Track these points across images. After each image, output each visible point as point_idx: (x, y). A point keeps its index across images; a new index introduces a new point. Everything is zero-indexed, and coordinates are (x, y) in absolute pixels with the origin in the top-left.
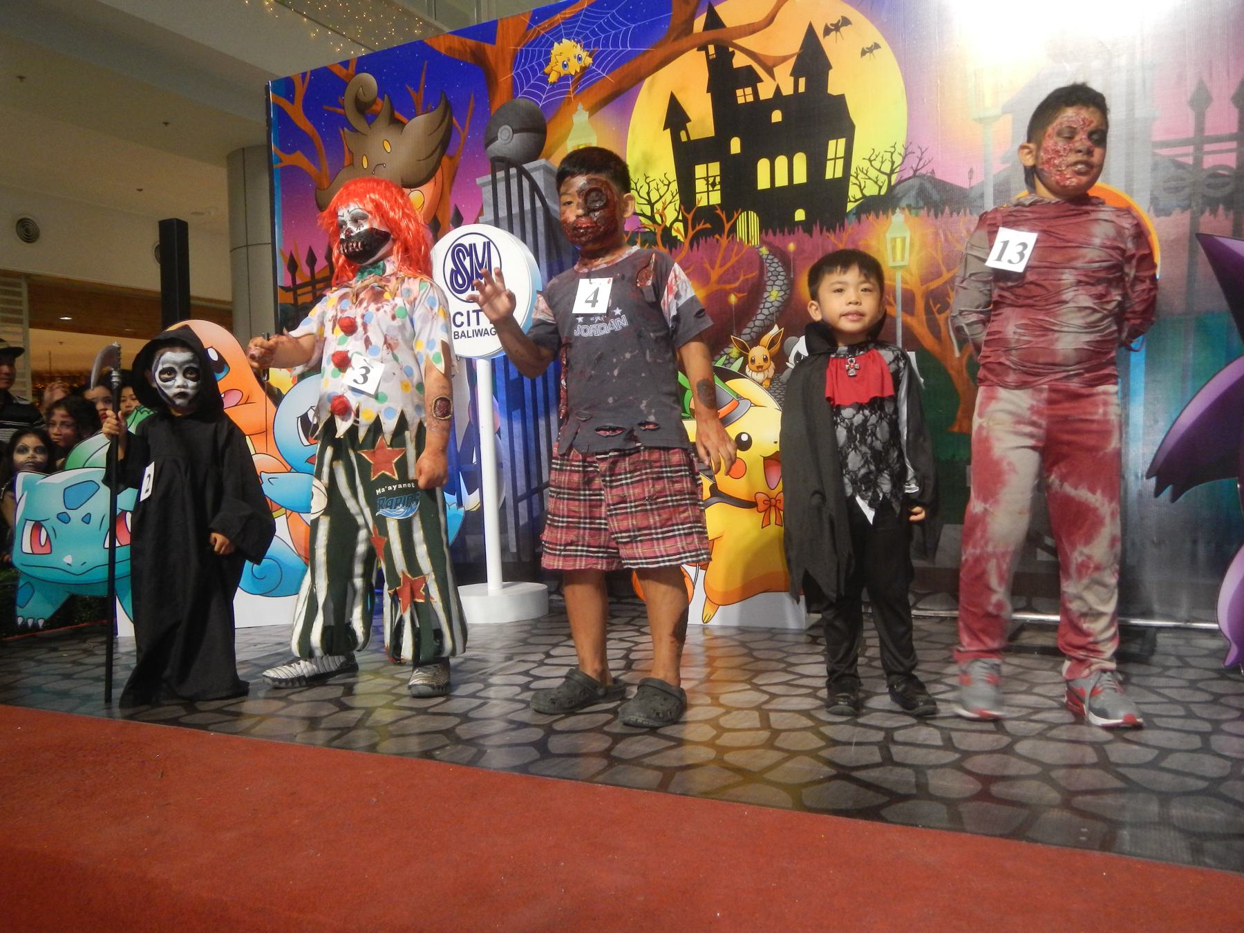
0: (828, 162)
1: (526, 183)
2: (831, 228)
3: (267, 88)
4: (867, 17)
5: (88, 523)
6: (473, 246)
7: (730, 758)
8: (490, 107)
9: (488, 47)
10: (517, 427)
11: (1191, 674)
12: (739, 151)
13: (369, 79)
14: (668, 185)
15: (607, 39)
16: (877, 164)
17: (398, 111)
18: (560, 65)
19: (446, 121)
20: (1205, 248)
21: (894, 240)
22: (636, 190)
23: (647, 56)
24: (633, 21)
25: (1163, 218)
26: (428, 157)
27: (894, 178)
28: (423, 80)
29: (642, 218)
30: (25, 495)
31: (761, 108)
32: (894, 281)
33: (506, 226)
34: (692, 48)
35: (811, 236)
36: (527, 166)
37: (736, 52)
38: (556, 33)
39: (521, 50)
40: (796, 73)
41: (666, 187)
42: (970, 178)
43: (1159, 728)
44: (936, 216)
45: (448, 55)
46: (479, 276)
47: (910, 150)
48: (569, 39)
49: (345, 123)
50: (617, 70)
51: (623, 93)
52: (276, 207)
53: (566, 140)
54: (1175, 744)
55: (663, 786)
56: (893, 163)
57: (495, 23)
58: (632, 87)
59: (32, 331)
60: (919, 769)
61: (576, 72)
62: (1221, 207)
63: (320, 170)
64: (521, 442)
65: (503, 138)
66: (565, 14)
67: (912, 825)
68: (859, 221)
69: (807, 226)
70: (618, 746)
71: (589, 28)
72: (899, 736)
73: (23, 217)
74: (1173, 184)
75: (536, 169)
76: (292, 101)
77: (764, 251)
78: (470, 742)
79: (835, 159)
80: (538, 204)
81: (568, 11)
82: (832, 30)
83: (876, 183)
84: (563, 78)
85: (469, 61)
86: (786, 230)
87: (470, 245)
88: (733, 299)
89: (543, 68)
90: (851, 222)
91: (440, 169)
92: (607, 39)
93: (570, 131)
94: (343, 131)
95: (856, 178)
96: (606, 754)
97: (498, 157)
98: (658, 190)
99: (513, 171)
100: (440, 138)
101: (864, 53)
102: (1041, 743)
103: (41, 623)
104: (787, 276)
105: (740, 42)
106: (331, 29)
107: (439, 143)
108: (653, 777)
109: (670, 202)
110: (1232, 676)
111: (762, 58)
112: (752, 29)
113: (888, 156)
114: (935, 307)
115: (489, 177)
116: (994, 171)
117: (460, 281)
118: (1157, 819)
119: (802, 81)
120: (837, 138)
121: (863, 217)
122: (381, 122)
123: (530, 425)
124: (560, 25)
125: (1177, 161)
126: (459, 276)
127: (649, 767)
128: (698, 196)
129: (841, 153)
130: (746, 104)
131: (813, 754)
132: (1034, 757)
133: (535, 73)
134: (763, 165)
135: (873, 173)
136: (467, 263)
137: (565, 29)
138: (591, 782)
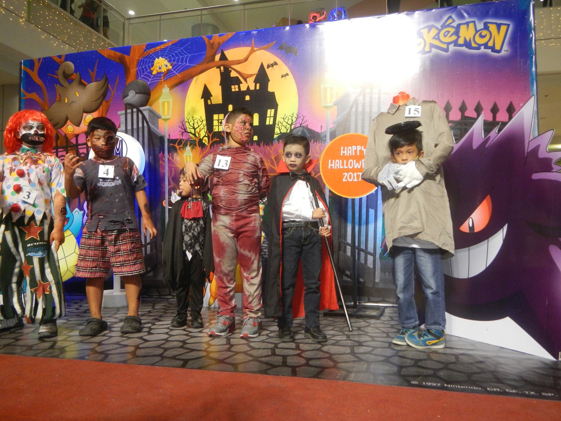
1: (140, 116)
2: (268, 144)
3: (21, 63)
4: (284, 63)
8: (126, 81)
9: (126, 56)
13: (71, 65)
14: (202, 122)
15: (179, 59)
16: (286, 120)
17: (83, 79)
18: (158, 68)
22: (188, 122)
23: (195, 68)
28: (96, 67)
29: (190, 135)
31: (241, 94)
33: (131, 133)
35: (260, 146)
36: (141, 108)
37: (232, 70)
38: (156, 55)
39: (141, 60)
40: (256, 82)
42: (321, 129)
43: (375, 341)
45: (108, 58)
47: (299, 116)
48: (162, 57)
49: (58, 82)
50: (182, 72)
51: (185, 81)
53: (158, 98)
56: (292, 120)
57: (130, 47)
58: (188, 79)
60: (285, 357)
61: (165, 71)
65: (131, 95)
66: (161, 47)
67: (278, 375)
68: (279, 143)
69: (258, 143)
70: (166, 352)
71: (171, 54)
72: (279, 346)
75: (145, 110)
76: (33, 70)
78: (102, 353)
79: (270, 117)
80: (145, 125)
82: (271, 66)
83: (286, 128)
85: (118, 62)
89: (150, 68)
90: (275, 142)
92: (179, 59)
93: (160, 96)
94: (57, 85)
96: (161, 355)
100: (102, 93)
101: (282, 77)
105: (234, 67)
106: (52, 35)
108: (181, 363)
111: (243, 74)
112: (239, 62)
115: (124, 112)
116: (330, 127)
119: (258, 85)
120: (271, 109)
122: (75, 84)
124: (158, 51)
128: (214, 127)
129: (272, 115)
130: (235, 92)
131: (245, 353)
132: (329, 352)
133: (147, 70)
135: (285, 124)
137: (161, 53)
138: (153, 365)
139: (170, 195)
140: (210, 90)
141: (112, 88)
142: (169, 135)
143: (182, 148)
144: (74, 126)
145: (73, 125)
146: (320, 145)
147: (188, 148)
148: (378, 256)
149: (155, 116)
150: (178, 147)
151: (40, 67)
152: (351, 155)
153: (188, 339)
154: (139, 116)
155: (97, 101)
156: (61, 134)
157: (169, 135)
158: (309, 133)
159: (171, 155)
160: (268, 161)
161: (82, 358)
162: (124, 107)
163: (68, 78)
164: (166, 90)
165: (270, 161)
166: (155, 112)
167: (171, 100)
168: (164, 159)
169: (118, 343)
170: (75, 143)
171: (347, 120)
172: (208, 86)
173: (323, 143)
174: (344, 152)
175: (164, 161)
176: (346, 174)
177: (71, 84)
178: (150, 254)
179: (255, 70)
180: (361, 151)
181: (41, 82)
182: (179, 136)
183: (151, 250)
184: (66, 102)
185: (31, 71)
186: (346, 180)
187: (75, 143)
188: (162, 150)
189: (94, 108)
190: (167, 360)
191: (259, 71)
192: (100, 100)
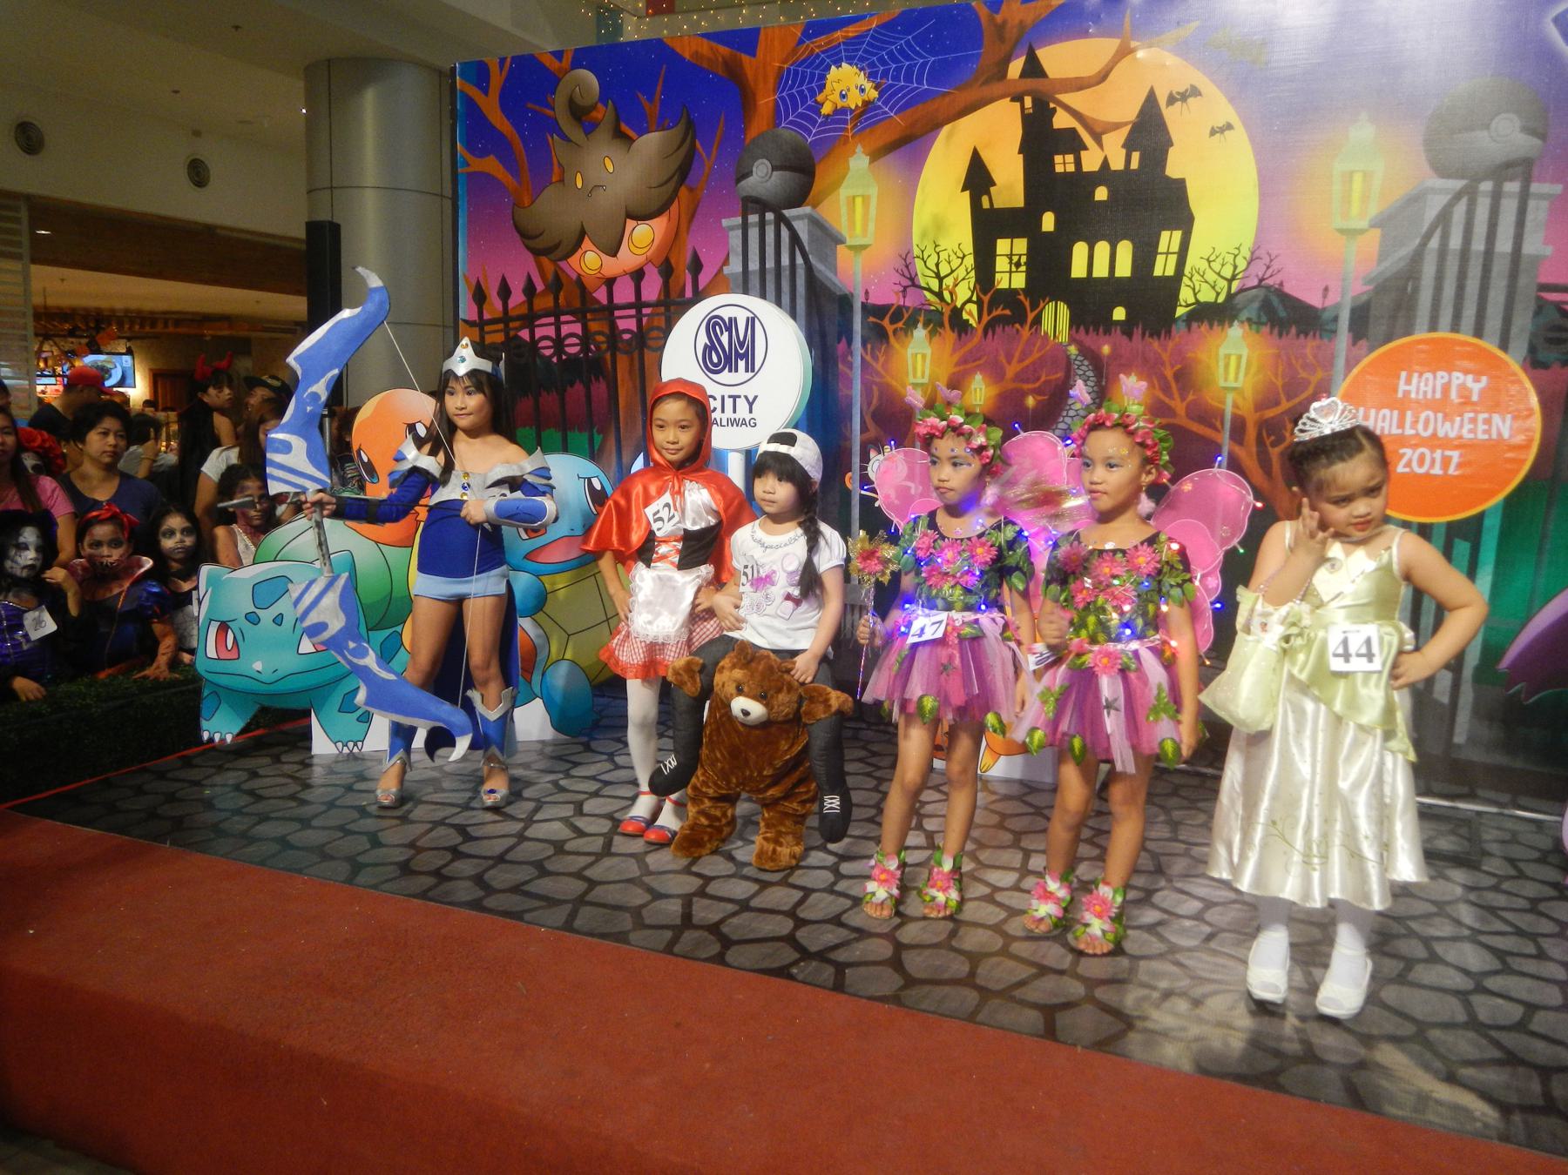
0: (1159, 257)
1: (785, 233)
2: (1155, 334)
6: (733, 321)
7: (1100, 993)
8: (744, 131)
9: (745, 58)
11: (1531, 889)
13: (589, 80)
14: (963, 258)
15: (898, 70)
16: (1216, 266)
17: (627, 124)
21: (1228, 357)
23: (947, 99)
24: (931, 53)
25: (1540, 372)
27: (1235, 286)
28: (659, 89)
29: (927, 294)
31: (1082, 182)
32: (1224, 403)
36: (787, 213)
37: (1058, 109)
38: (832, 56)
39: (789, 69)
40: (1129, 146)
42: (1325, 296)
44: (1280, 335)
46: (741, 357)
50: (909, 111)
52: (462, 221)
53: (837, 185)
54: (1535, 998)
55: (1050, 1032)
56: (1235, 267)
58: (927, 133)
59: (34, 268)
68: (1189, 327)
69: (1127, 327)
73: (26, 119)
74: (1557, 335)
75: (799, 218)
76: (486, 92)
77: (1073, 350)
79: (1168, 253)
80: (799, 260)
81: (851, 28)
82: (1177, 100)
83: (1213, 288)
84: (840, 112)
85: (720, 73)
87: (730, 319)
88: (1030, 401)
91: (676, 202)
92: (898, 70)
96: (969, 981)
99: (770, 216)
101: (1213, 132)
102: (1405, 990)
103: (229, 738)
104: (1098, 383)
105: (1064, 98)
108: (1032, 1018)
112: (1079, 85)
113: (1230, 258)
114: (1269, 435)
115: (739, 220)
117: (715, 359)
118: (1541, 1102)
119: (1136, 156)
120: (1172, 228)
122: (603, 134)
127: (1024, 1003)
128: (998, 276)
129: (1175, 247)
130: (1065, 174)
134: (1080, 250)
135: (1211, 277)
136: (725, 339)
138: (975, 1023)
139: (865, 459)
140: (990, 167)
142: (867, 292)
143: (901, 334)
144: (604, 256)
147: (920, 333)
148: (1468, 672)
149: (829, 237)
150: (890, 328)
151: (506, 81)
152: (1429, 396)
153: (1005, 921)
155: (664, 188)
157: (867, 292)
158: (1285, 307)
159: (872, 349)
164: (859, 162)
167: (873, 192)
169: (837, 921)
170: (605, 302)
171: (1411, 271)
172: (985, 156)
173: (1326, 340)
174: (1407, 388)
175: (850, 366)
176: (1408, 452)
179: (1129, 111)
180: (1464, 392)
184: (579, 185)
186: (1407, 470)
188: (846, 332)
190: (997, 1001)
191: (1142, 113)
192: (672, 185)
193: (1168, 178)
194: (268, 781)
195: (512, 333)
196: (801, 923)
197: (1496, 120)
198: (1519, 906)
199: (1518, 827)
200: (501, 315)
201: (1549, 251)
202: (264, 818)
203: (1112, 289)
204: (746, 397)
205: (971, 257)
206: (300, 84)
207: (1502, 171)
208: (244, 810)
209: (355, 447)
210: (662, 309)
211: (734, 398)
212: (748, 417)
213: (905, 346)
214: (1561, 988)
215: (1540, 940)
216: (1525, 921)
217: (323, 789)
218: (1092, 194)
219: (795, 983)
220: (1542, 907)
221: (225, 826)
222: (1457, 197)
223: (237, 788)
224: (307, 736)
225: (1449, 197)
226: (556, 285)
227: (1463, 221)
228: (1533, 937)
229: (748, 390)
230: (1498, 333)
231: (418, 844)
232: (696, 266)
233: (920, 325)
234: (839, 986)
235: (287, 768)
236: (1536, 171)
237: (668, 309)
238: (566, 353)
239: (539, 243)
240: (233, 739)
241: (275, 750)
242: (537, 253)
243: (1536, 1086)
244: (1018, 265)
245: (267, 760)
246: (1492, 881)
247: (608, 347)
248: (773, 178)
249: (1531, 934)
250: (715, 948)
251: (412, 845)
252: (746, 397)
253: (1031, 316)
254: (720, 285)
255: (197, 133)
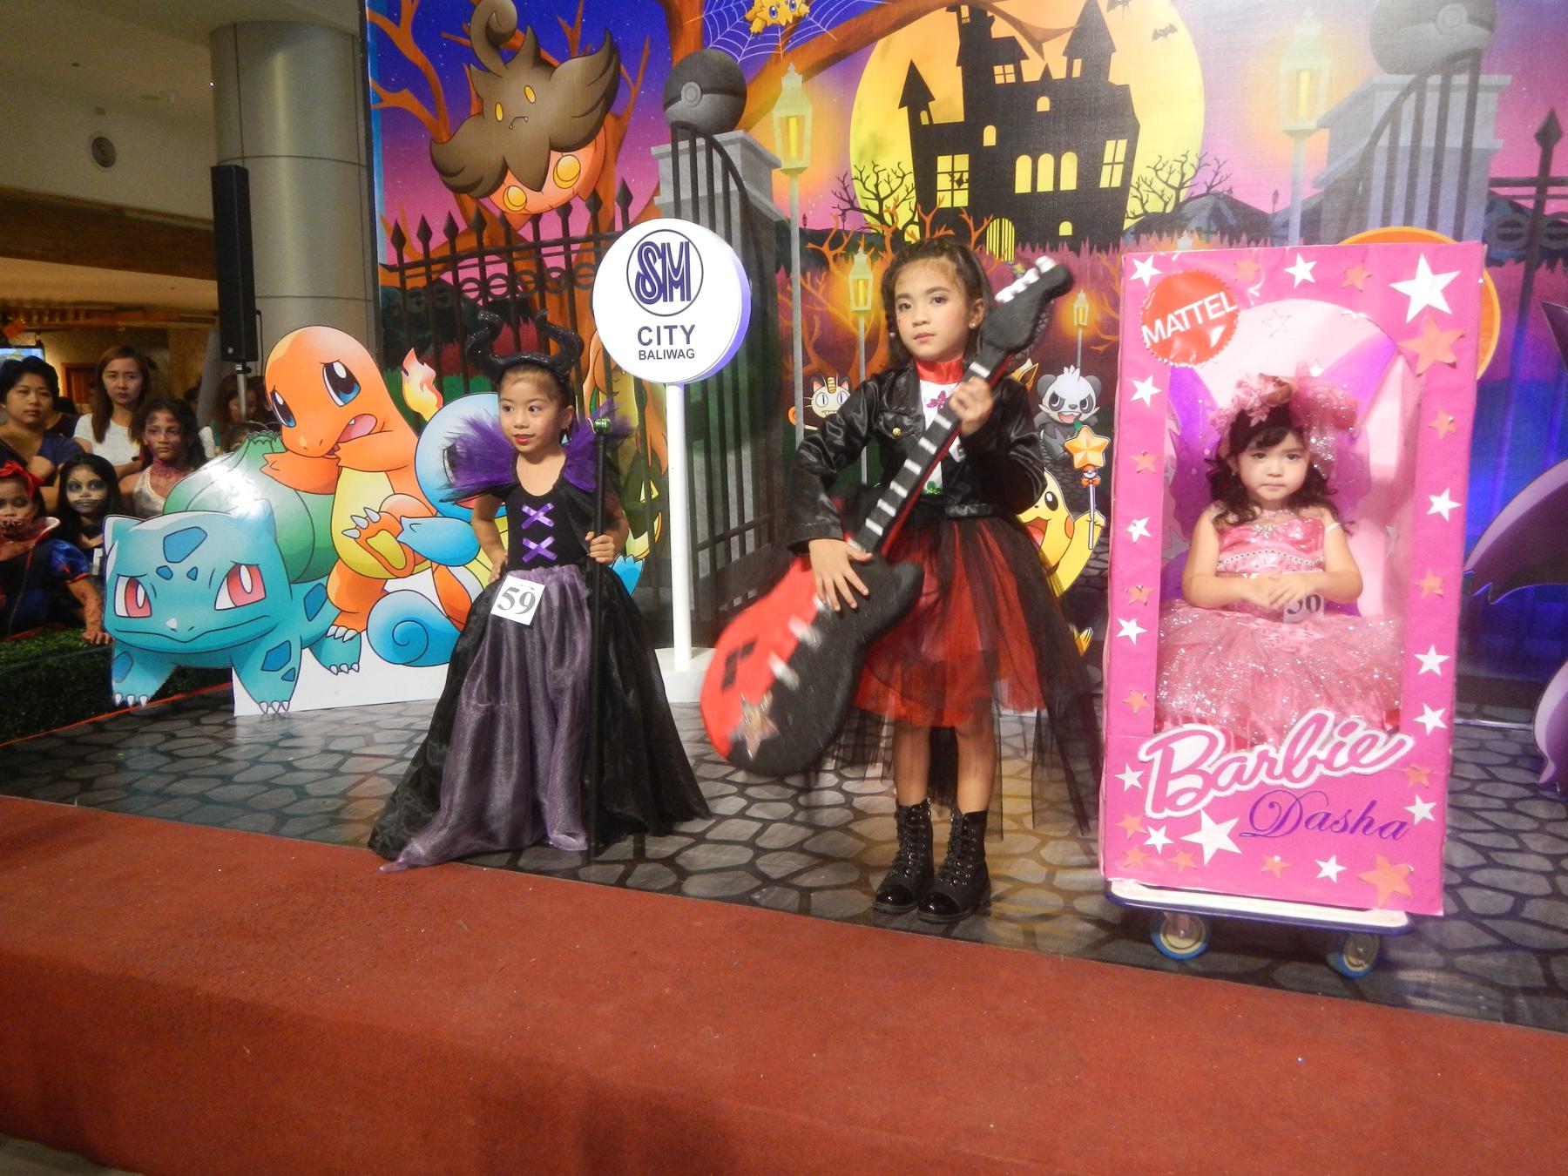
1: (717, 159)
2: (1103, 248)
5: (195, 579)
8: (670, 54)
10: (699, 461)
11: (1506, 791)
12: (994, 144)
14: (903, 178)
16: (1163, 175)
17: (547, 50)
19: (611, 69)
20: (1551, 320)
26: (587, 113)
27: (1184, 194)
28: (580, 12)
29: (866, 216)
30: (117, 543)
31: (1024, 92)
34: (939, 7)
35: (1078, 254)
36: (719, 138)
37: (996, 17)
40: (1071, 53)
41: (900, 180)
42: (1275, 202)
44: (1231, 245)
46: (676, 284)
47: (1206, 159)
49: (472, 57)
50: (842, 26)
51: (851, 54)
52: (375, 161)
54: (1524, 889)
56: (1183, 175)
58: (860, 48)
61: (787, 22)
62: (1560, 261)
63: (436, 116)
64: (704, 478)
68: (1138, 239)
69: (1074, 243)
74: (1509, 230)
75: (731, 142)
76: (397, 21)
79: (1113, 164)
80: (733, 187)
83: (1161, 197)
86: (1048, 246)
87: (663, 245)
90: (1129, 239)
93: (775, 99)
94: (469, 68)
95: (1138, 189)
97: (682, 122)
98: (889, 183)
99: (701, 142)
101: (1156, 35)
103: (144, 700)
107: (602, 97)
109: (904, 200)
110: (1548, 794)
113: (1177, 166)
115: (668, 147)
117: (649, 289)
118: (1544, 984)
119: (1078, 64)
120: (1117, 138)
121: (1143, 237)
122: (522, 64)
123: (716, 459)
125: (1516, 204)
126: (647, 281)
128: (940, 195)
129: (1121, 157)
130: (1006, 84)
133: (732, 19)
134: (1023, 164)
135: (1158, 186)
136: (658, 266)
138: (949, 937)
139: (809, 392)
141: (630, 76)
142: (805, 218)
144: (527, 191)
145: (521, 186)
146: (1269, 248)
147: (861, 257)
149: (763, 161)
150: (830, 254)
151: (416, 14)
154: (714, 159)
156: (490, 212)
157: (805, 218)
158: (1235, 215)
159: (812, 279)
160: (1102, 299)
161: (745, 899)
162: (670, 133)
163: (502, 47)
164: (791, 81)
165: (1108, 298)
166: (760, 149)
167: (808, 112)
168: (789, 288)
170: (530, 238)
175: (790, 296)
177: (512, 62)
178: (753, 554)
179: (1069, 17)
181: (425, 59)
182: (833, 219)
183: (758, 543)
184: (500, 117)
185: (394, 25)
187: (530, 238)
188: (784, 261)
189: (582, 135)
193: (1112, 85)
194: (187, 742)
195: (434, 277)
196: (761, 852)
197: (1441, 14)
198: (1497, 807)
199: (1484, 735)
200: (421, 257)
201: (1499, 144)
202: (182, 776)
203: (1058, 203)
204: (683, 327)
205: (912, 176)
206: (204, 54)
207: (1450, 64)
208: (161, 770)
209: (269, 389)
210: (592, 244)
211: (671, 328)
212: (685, 348)
213: (845, 272)
214: (1548, 879)
215: (1522, 836)
216: (1502, 819)
217: (247, 747)
218: (1034, 105)
219: (756, 909)
220: (1518, 806)
221: (137, 785)
222: (1406, 92)
223: (154, 749)
224: (229, 699)
225: (1397, 93)
226: (479, 224)
227: (1413, 117)
228: (1514, 833)
229: (684, 320)
230: (1452, 230)
231: (350, 794)
232: (626, 197)
233: (861, 250)
234: (804, 910)
235: (206, 730)
236: (1484, 63)
237: (597, 244)
238: (493, 296)
239: (457, 181)
240: (152, 700)
241: (192, 714)
242: (457, 190)
243: (1537, 969)
244: (960, 182)
245: (187, 723)
246: (1467, 785)
247: (536, 288)
248: (703, 102)
249: (1511, 830)
250: (672, 879)
251: (343, 795)
252: (683, 327)
253: (975, 235)
254: (650, 212)
255: (100, 111)
